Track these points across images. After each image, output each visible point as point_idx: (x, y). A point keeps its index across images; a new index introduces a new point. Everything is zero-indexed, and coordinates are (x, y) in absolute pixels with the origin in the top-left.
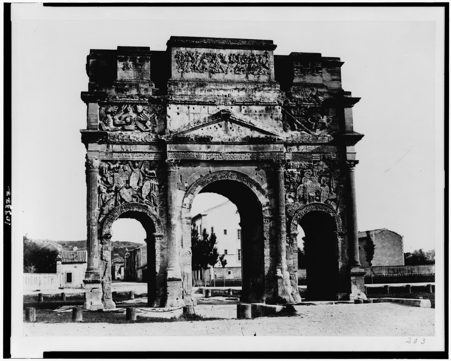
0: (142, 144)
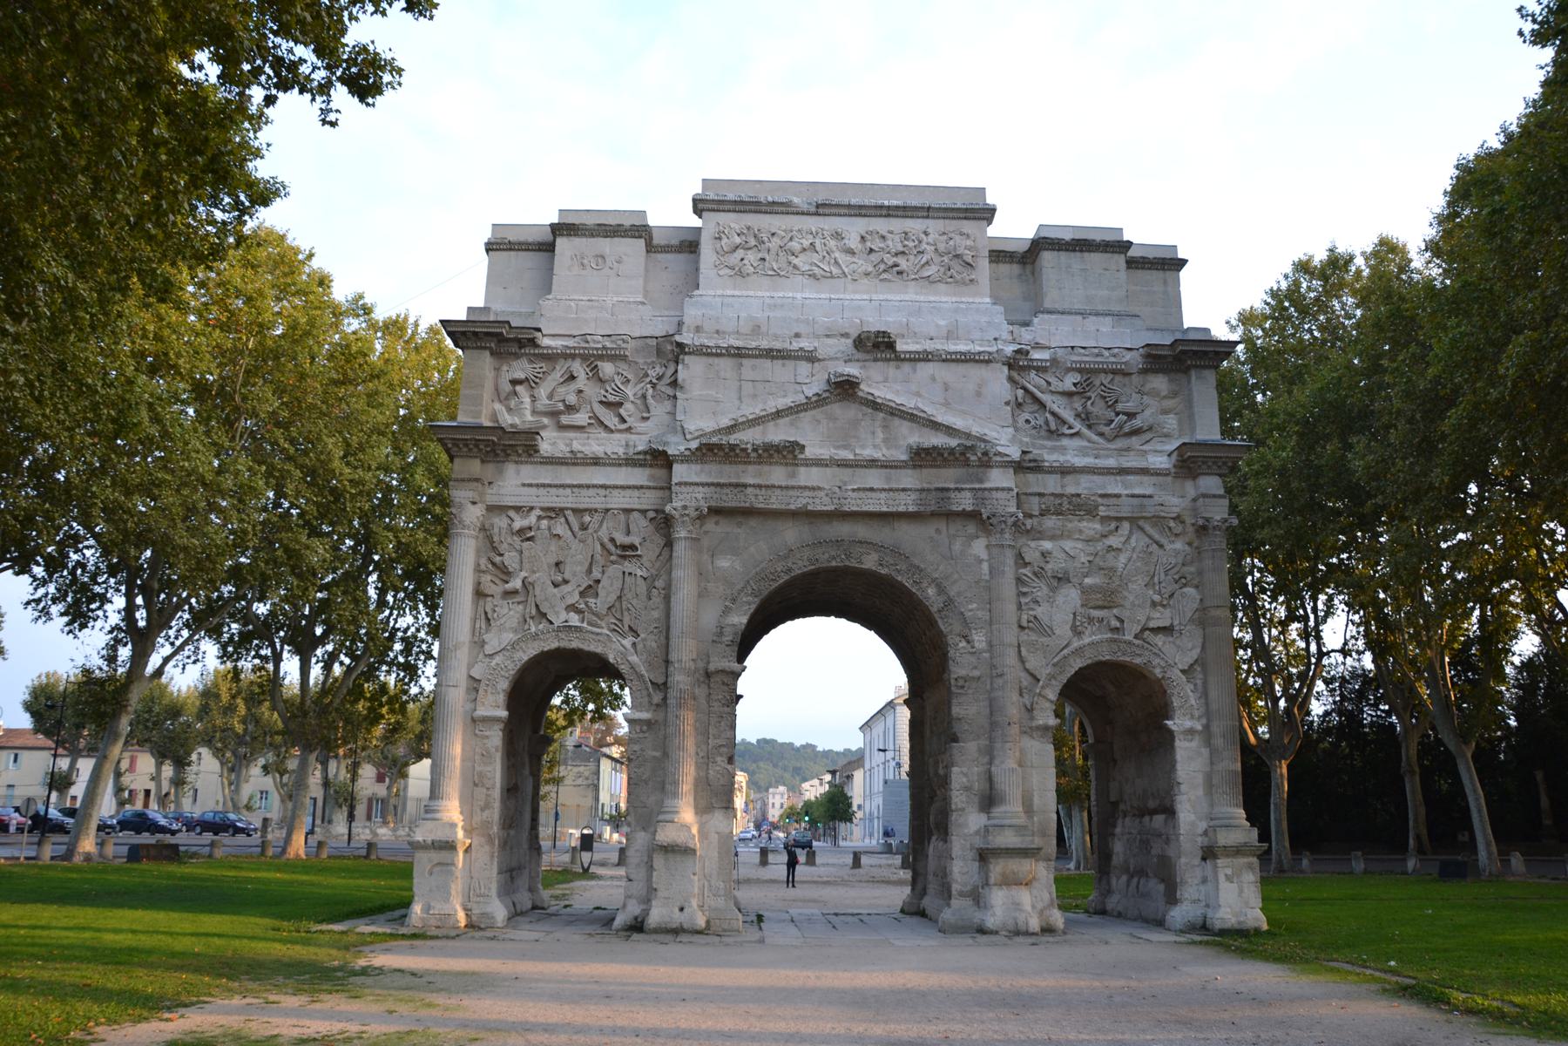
0: (605, 465)
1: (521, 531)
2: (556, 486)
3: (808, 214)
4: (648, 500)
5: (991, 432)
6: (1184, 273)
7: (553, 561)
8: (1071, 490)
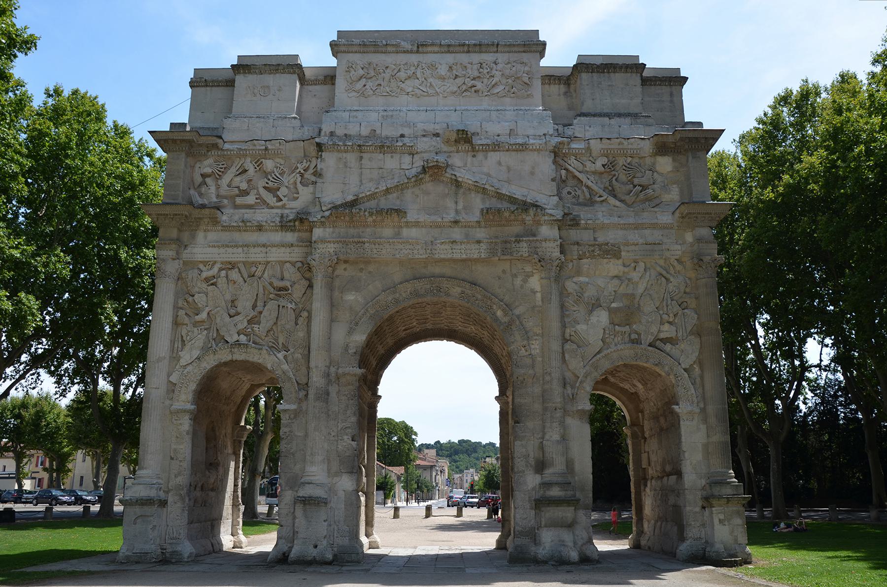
1: (207, 280)
2: (231, 246)
3: (411, 52)
4: (296, 254)
5: (542, 200)
6: (686, 89)
7: (228, 297)
8: (601, 240)
